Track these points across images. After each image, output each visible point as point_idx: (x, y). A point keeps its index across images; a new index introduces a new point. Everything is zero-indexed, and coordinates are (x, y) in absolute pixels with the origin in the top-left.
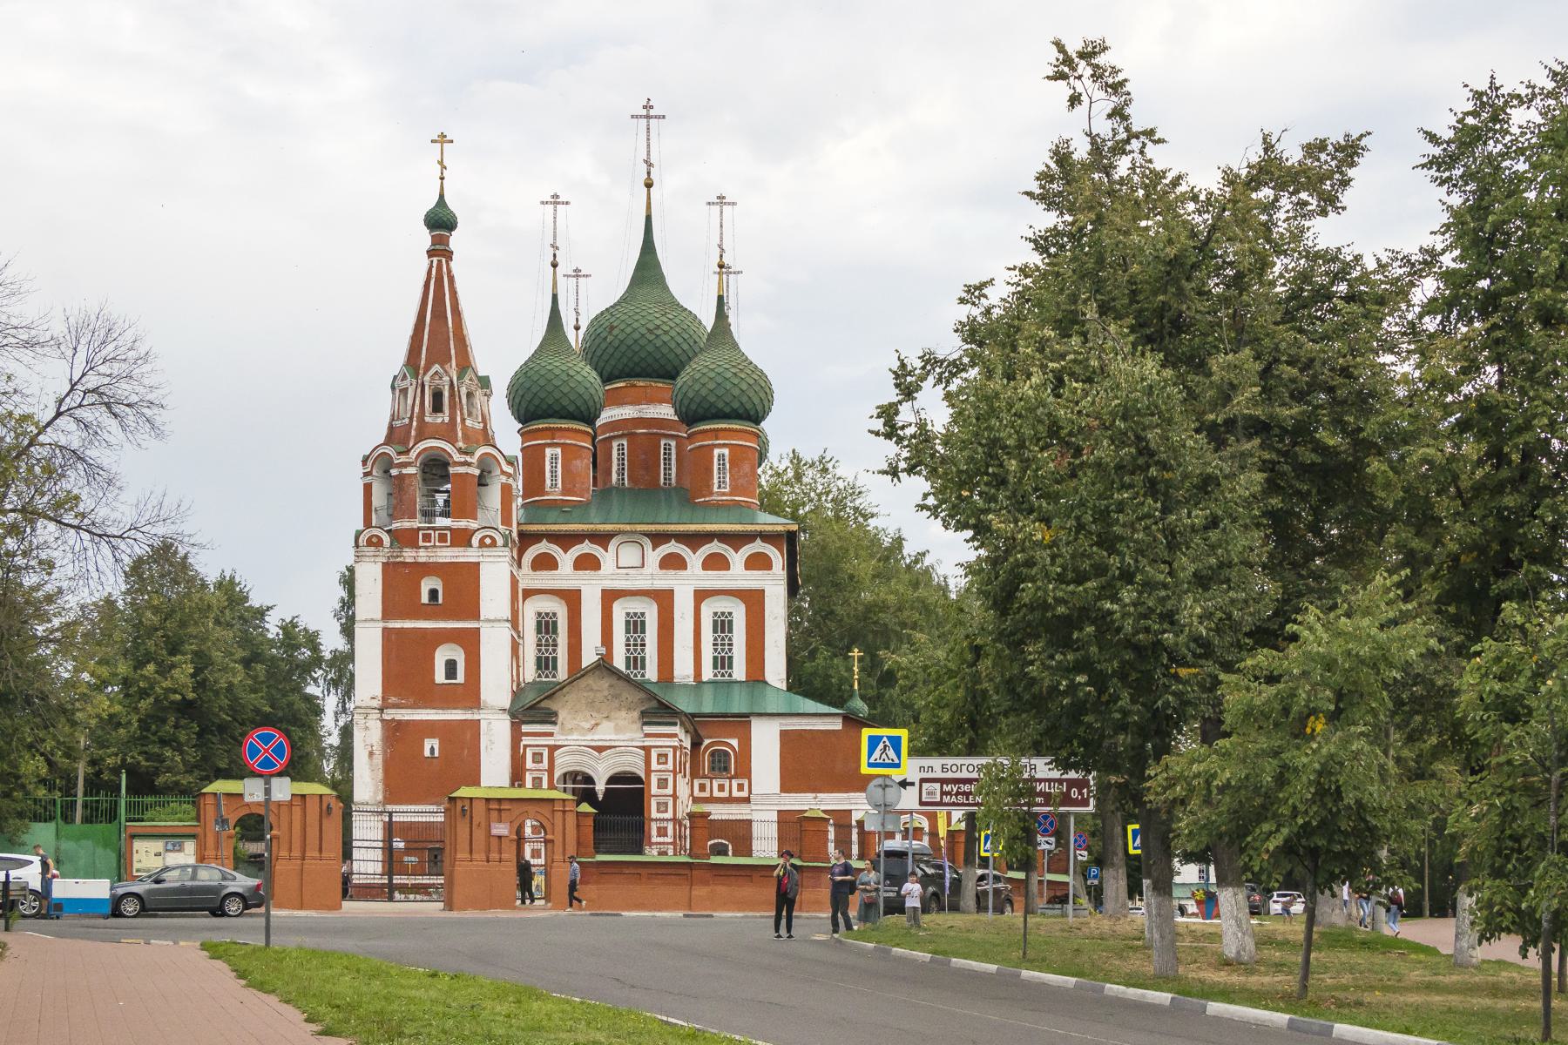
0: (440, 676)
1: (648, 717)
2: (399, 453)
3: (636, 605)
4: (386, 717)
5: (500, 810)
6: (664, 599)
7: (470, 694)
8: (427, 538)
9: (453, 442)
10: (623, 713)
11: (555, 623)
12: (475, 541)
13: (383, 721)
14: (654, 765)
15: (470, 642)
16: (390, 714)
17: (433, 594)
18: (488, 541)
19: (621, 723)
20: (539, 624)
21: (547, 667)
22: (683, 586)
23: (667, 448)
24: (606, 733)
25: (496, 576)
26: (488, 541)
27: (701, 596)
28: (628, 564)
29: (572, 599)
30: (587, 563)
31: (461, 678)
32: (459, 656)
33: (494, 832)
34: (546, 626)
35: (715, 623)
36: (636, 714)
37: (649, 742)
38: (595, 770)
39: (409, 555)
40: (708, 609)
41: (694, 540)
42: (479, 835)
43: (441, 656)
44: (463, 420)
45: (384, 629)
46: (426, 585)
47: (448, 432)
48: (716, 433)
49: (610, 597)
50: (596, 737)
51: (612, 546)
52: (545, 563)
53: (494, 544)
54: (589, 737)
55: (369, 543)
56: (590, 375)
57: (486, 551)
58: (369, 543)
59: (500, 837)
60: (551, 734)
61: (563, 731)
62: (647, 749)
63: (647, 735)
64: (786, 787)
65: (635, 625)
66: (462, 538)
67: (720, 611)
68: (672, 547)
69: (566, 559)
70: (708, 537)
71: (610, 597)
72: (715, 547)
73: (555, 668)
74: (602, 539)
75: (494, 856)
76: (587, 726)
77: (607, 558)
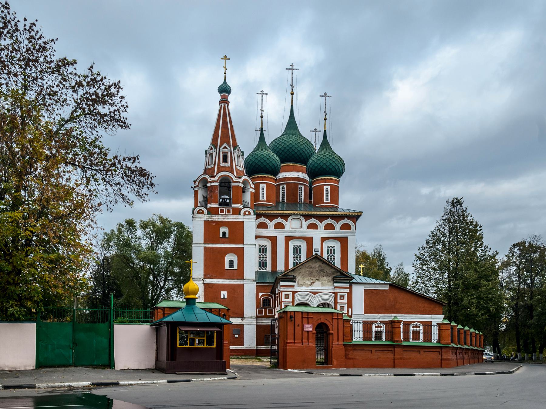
0: (227, 267)
1: (336, 280)
2: (211, 177)
3: (297, 243)
4: (205, 282)
5: (308, 318)
6: (309, 241)
7: (240, 274)
8: (222, 211)
9: (232, 172)
10: (325, 278)
11: (266, 249)
12: (242, 213)
13: (204, 284)
14: (339, 301)
15: (240, 253)
16: (208, 281)
17: (224, 234)
18: (247, 213)
19: (324, 282)
20: (260, 249)
21: (263, 266)
22: (317, 235)
23: (301, 189)
24: (317, 286)
25: (250, 226)
26: (247, 213)
27: (323, 239)
28: (295, 227)
29: (273, 240)
30: (279, 226)
31: (235, 267)
32: (235, 258)
33: (305, 329)
34: (262, 250)
35: (328, 250)
36: (330, 278)
37: (336, 290)
38: (312, 302)
39: (215, 218)
40: (326, 244)
41: (321, 218)
42: (298, 329)
43: (228, 258)
44: (236, 166)
45: (205, 248)
46: (222, 230)
47: (231, 170)
48: (325, 181)
49: (288, 239)
50: (313, 288)
51: (290, 219)
52: (262, 226)
53: (249, 214)
54: (310, 288)
55: (199, 213)
56: (276, 158)
57: (247, 217)
58: (199, 213)
59: (308, 332)
60: (293, 286)
61: (299, 285)
62: (335, 294)
63: (335, 287)
64: (366, 312)
65: (298, 250)
66: (237, 212)
67: (330, 245)
68: (313, 221)
69: (271, 224)
70: (327, 217)
71: (288, 239)
72: (329, 221)
73: (266, 266)
74: (285, 217)
75: (305, 341)
76: (309, 283)
77: (287, 224)
